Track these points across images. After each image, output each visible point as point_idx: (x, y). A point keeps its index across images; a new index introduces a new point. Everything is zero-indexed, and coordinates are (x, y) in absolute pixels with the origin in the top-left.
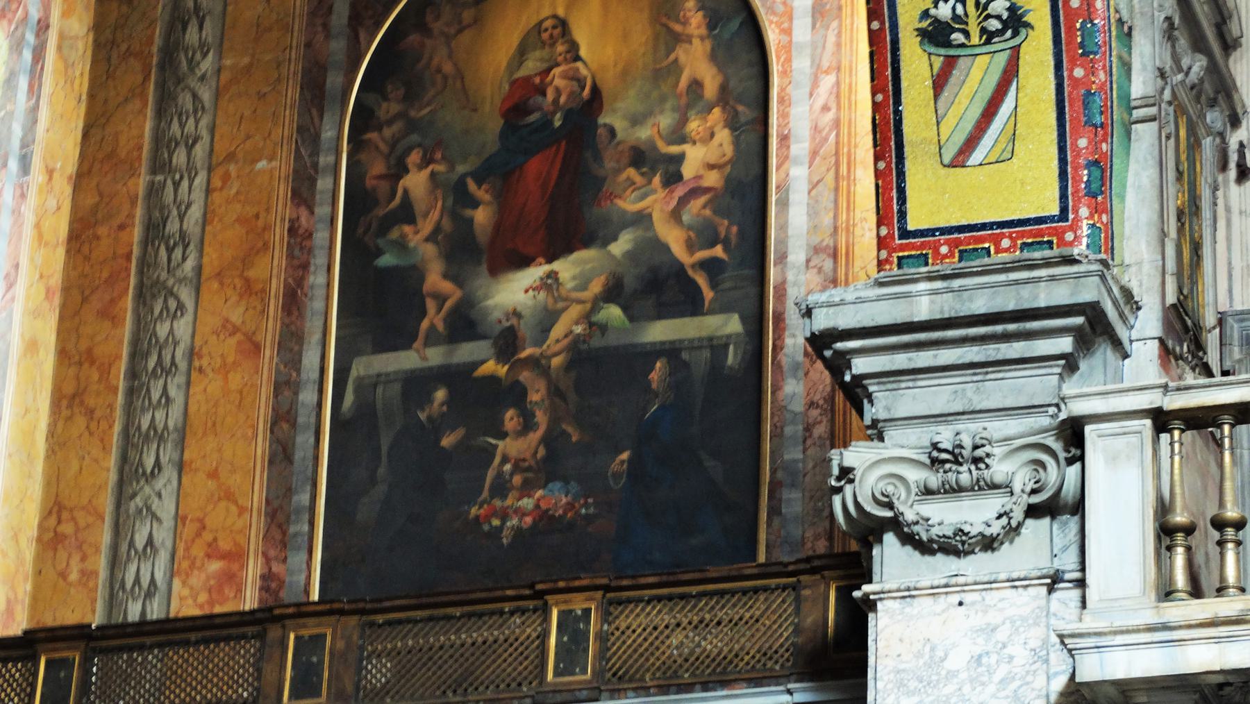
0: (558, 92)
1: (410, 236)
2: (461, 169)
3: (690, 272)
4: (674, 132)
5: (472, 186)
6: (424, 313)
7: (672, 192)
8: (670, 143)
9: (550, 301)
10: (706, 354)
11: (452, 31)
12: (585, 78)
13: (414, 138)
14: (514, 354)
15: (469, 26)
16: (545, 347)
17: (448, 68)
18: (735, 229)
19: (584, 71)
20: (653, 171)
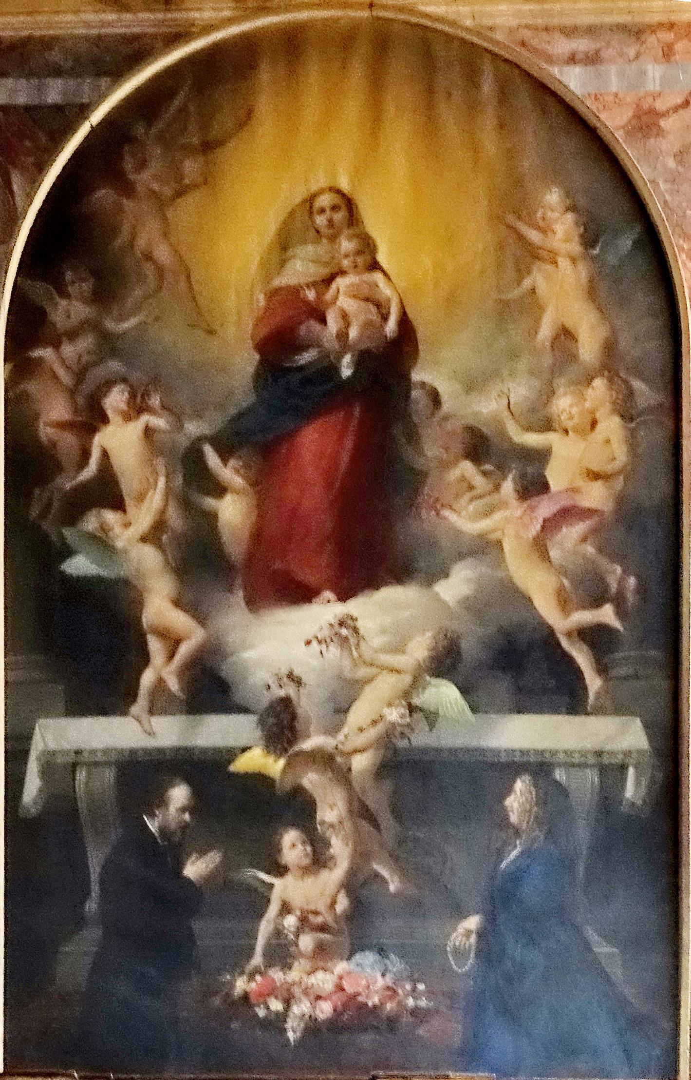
0: (345, 317)
1: (117, 530)
2: (193, 428)
3: (565, 643)
4: (533, 410)
5: (212, 459)
6: (145, 659)
7: (532, 509)
8: (529, 428)
9: (347, 663)
10: (592, 777)
11: (168, 191)
12: (389, 300)
13: (115, 366)
14: (291, 742)
15: (194, 186)
16: (341, 737)
17: (163, 253)
18: (632, 581)
19: (385, 290)
20: (502, 469)
